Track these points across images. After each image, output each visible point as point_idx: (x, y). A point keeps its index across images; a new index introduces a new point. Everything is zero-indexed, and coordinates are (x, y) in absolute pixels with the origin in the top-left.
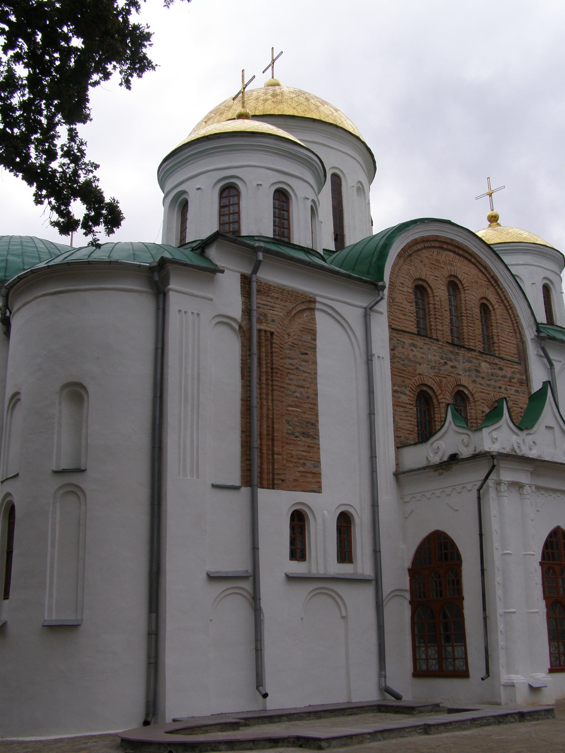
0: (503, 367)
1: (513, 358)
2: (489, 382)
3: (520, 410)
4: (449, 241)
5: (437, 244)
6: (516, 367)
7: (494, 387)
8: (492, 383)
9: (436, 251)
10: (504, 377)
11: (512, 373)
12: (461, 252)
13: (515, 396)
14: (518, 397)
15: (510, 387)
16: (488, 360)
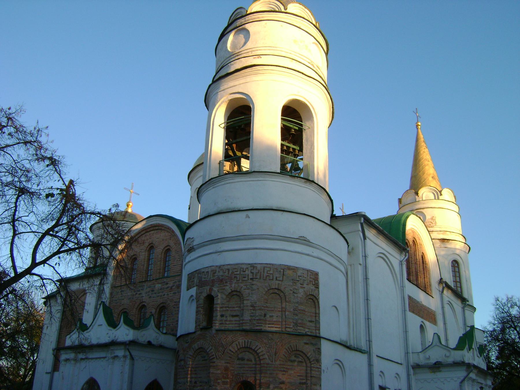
0: (168, 282)
1: (178, 274)
2: (158, 295)
3: (174, 304)
4: (150, 226)
5: (144, 232)
6: (177, 278)
7: (161, 296)
8: (161, 294)
9: (144, 236)
10: (168, 288)
11: (174, 283)
12: (157, 228)
13: (173, 297)
14: (174, 296)
15: (171, 292)
16: (160, 282)
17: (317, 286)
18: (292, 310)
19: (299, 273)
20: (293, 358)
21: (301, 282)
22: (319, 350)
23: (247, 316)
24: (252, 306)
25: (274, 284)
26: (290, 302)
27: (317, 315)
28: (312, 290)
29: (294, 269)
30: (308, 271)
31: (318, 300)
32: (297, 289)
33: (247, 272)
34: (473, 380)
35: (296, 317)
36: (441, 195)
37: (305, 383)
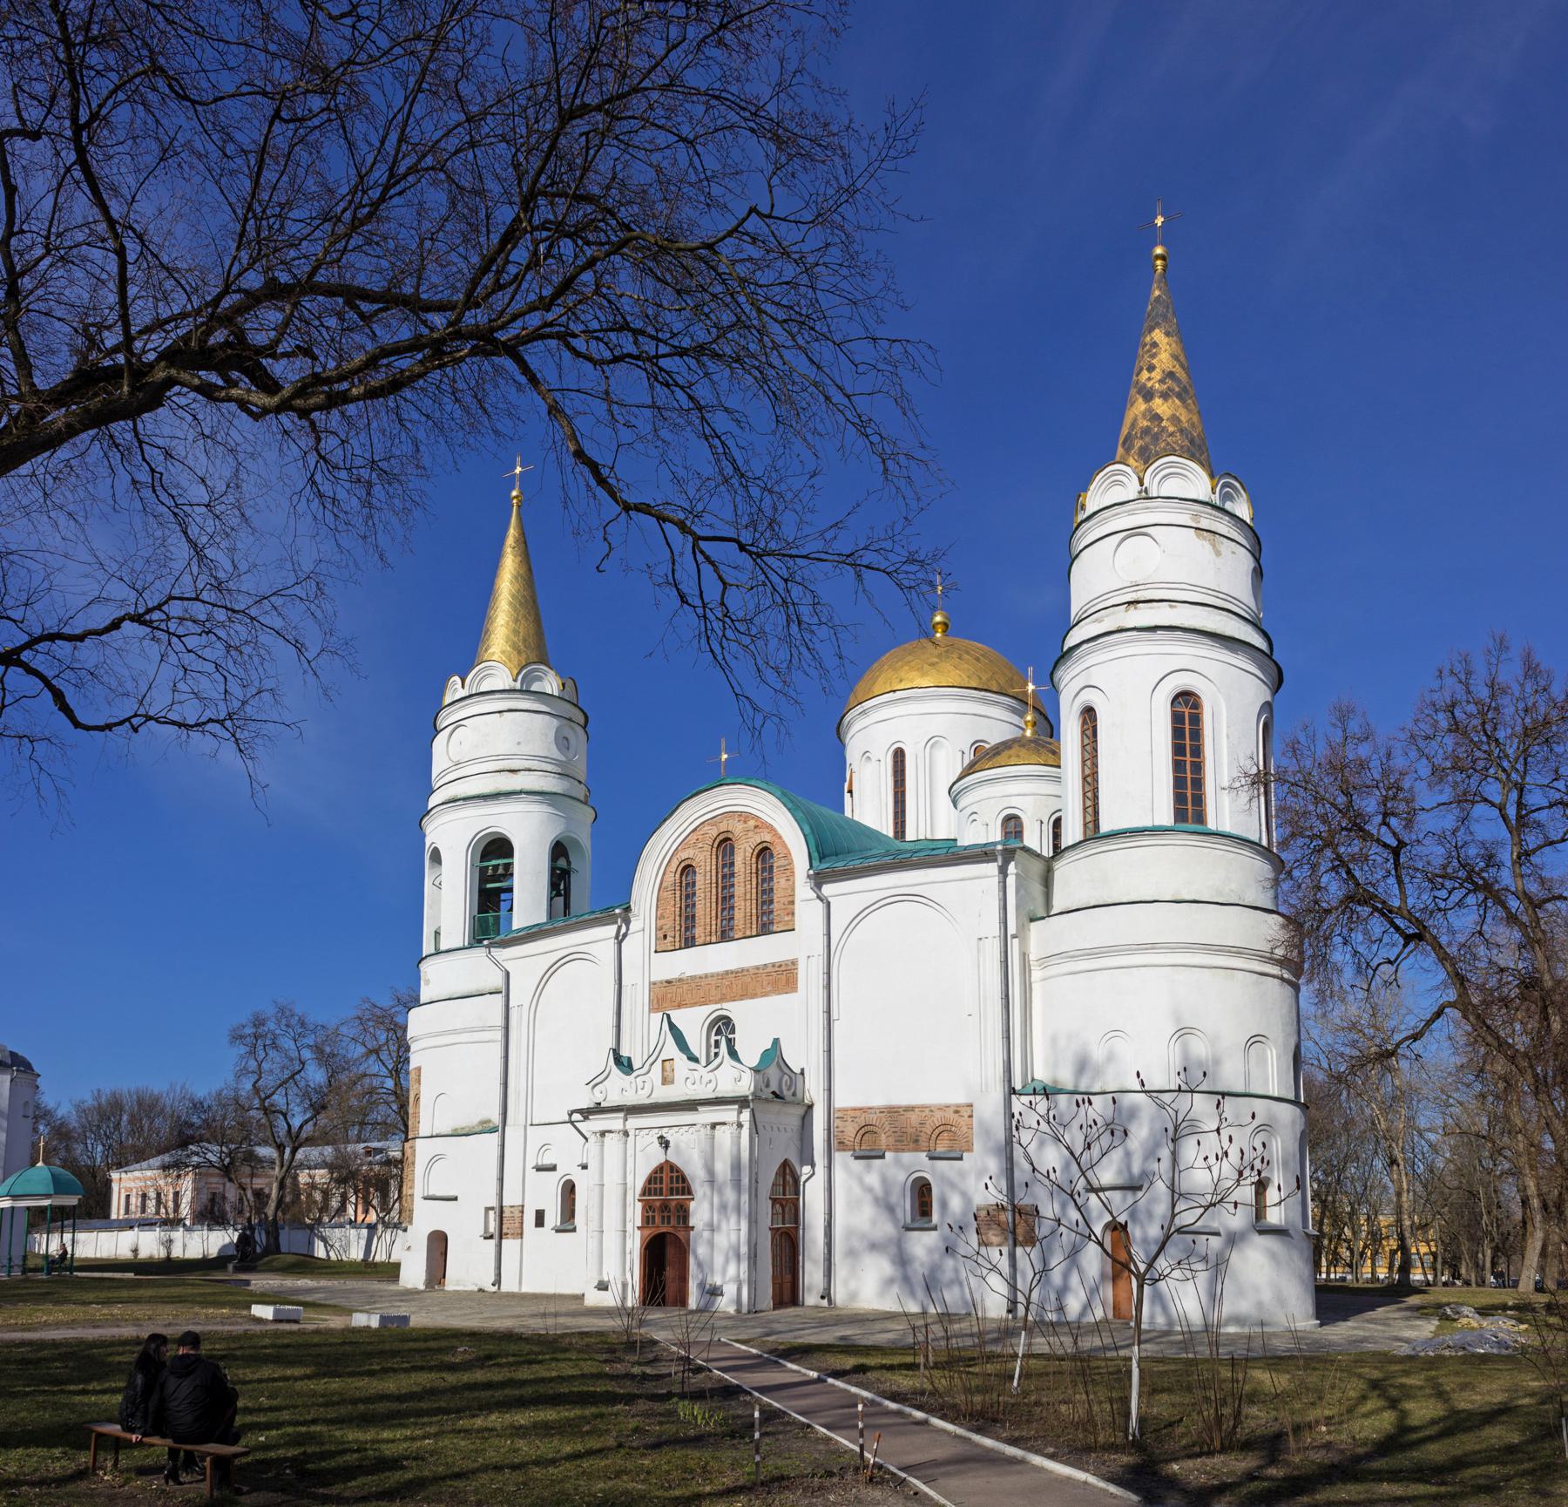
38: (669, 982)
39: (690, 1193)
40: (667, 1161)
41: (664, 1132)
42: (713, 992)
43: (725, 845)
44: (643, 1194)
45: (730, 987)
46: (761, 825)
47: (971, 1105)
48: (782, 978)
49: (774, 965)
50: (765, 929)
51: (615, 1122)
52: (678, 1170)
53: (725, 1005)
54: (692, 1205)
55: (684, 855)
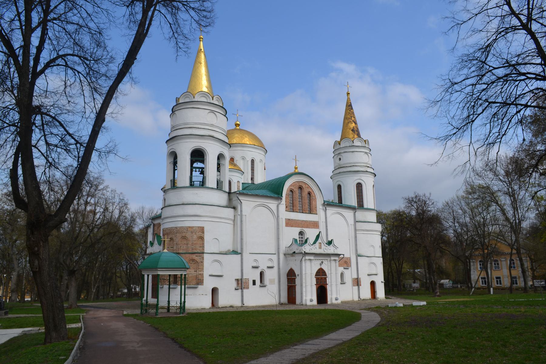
17: (203, 232)
18: (191, 244)
19: (194, 229)
20: (191, 262)
21: (195, 232)
22: (203, 258)
23: (175, 248)
24: (177, 244)
25: (184, 234)
26: (190, 241)
27: (203, 244)
28: (200, 235)
29: (192, 227)
30: (198, 227)
31: (203, 238)
32: (193, 235)
33: (175, 230)
34: (310, 260)
35: (193, 246)
36: (353, 143)
37: (196, 271)
38: (289, 219)
39: (326, 275)
40: (321, 268)
41: (323, 261)
42: (300, 225)
43: (301, 188)
44: (316, 276)
45: (304, 224)
46: (309, 187)
47: (350, 258)
48: (315, 225)
49: (313, 221)
50: (310, 212)
51: (312, 258)
52: (323, 270)
53: (303, 229)
54: (327, 279)
55: (292, 188)
